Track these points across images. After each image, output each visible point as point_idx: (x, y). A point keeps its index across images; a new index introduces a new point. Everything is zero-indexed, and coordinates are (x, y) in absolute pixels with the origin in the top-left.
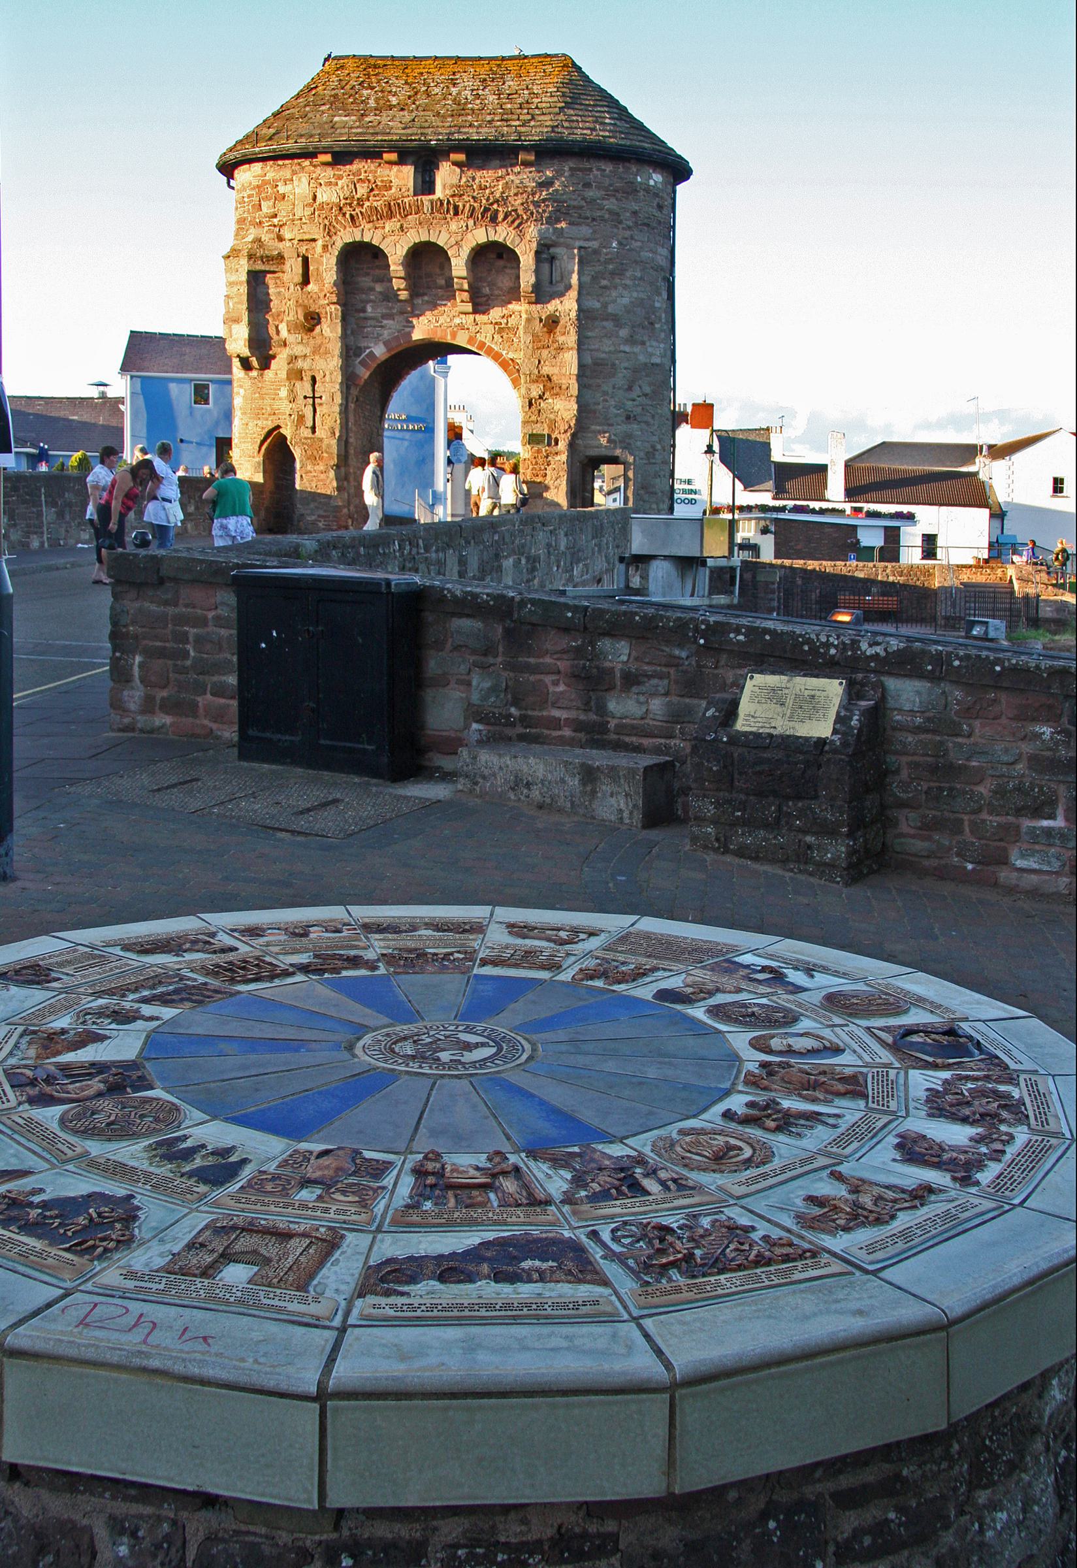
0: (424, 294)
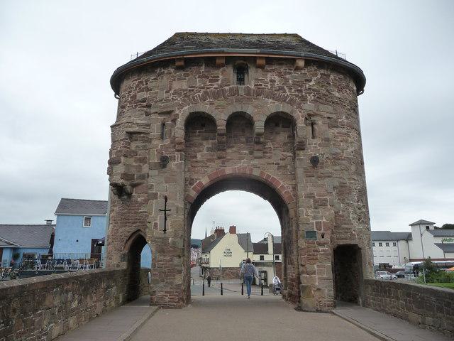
0: (233, 147)
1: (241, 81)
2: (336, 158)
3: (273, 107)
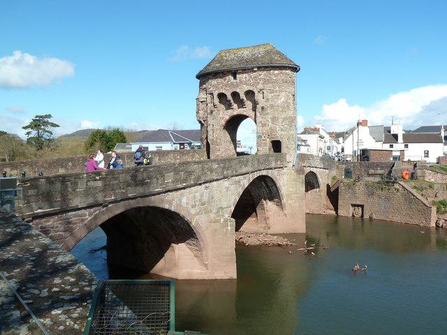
1: (235, 78)
2: (272, 106)
3: (246, 88)
